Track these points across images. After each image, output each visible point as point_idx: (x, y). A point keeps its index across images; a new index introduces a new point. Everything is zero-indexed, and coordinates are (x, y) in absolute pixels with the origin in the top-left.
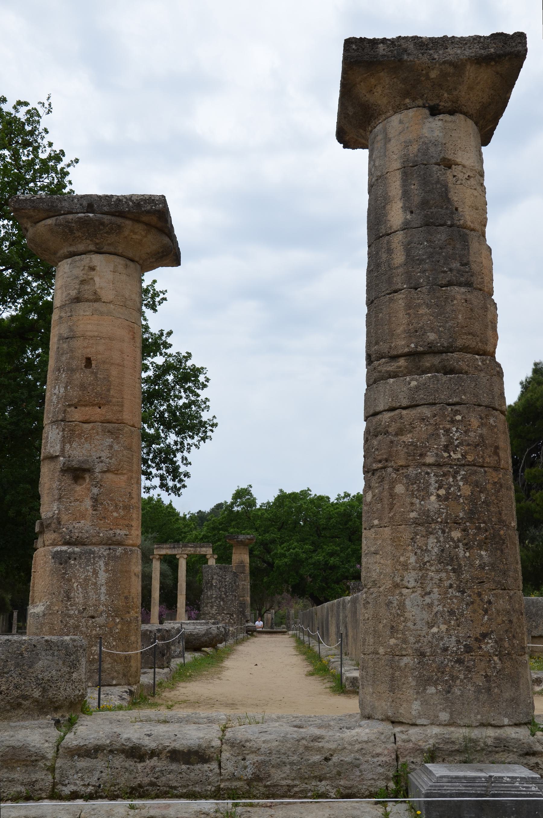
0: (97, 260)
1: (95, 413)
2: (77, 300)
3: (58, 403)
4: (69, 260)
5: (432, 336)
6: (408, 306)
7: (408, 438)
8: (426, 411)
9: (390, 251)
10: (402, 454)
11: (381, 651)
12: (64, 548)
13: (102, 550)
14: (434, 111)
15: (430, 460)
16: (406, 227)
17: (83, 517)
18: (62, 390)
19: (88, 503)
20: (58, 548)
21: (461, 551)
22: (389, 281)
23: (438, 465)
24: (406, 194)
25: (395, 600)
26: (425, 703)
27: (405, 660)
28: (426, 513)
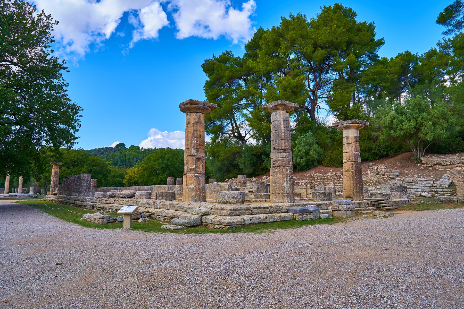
0: (201, 114)
2: (197, 123)
3: (194, 144)
4: (195, 113)
5: (288, 147)
6: (285, 143)
7: (284, 162)
8: (287, 159)
9: (281, 133)
10: (284, 164)
11: (280, 193)
12: (198, 175)
15: (288, 166)
16: (284, 130)
17: (200, 168)
18: (195, 142)
19: (201, 166)
20: (196, 175)
22: (281, 138)
23: (289, 167)
24: (284, 125)
25: (283, 186)
26: (288, 200)
27: (285, 194)
28: (287, 174)
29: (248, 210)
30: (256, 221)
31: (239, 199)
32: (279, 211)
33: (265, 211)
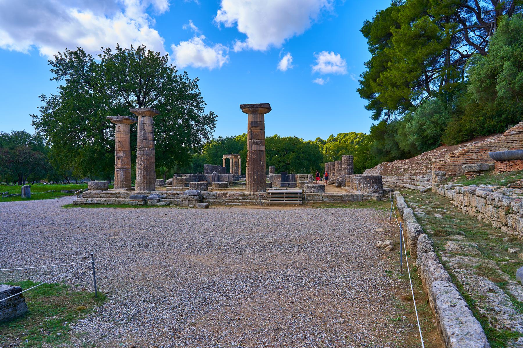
0: (120, 125)
1: (120, 149)
5: (141, 146)
8: (140, 156)
13: (122, 169)
14: (143, 116)
21: (143, 172)
29: (97, 194)
30: (96, 202)
31: (92, 187)
32: (127, 197)
33: (112, 196)
